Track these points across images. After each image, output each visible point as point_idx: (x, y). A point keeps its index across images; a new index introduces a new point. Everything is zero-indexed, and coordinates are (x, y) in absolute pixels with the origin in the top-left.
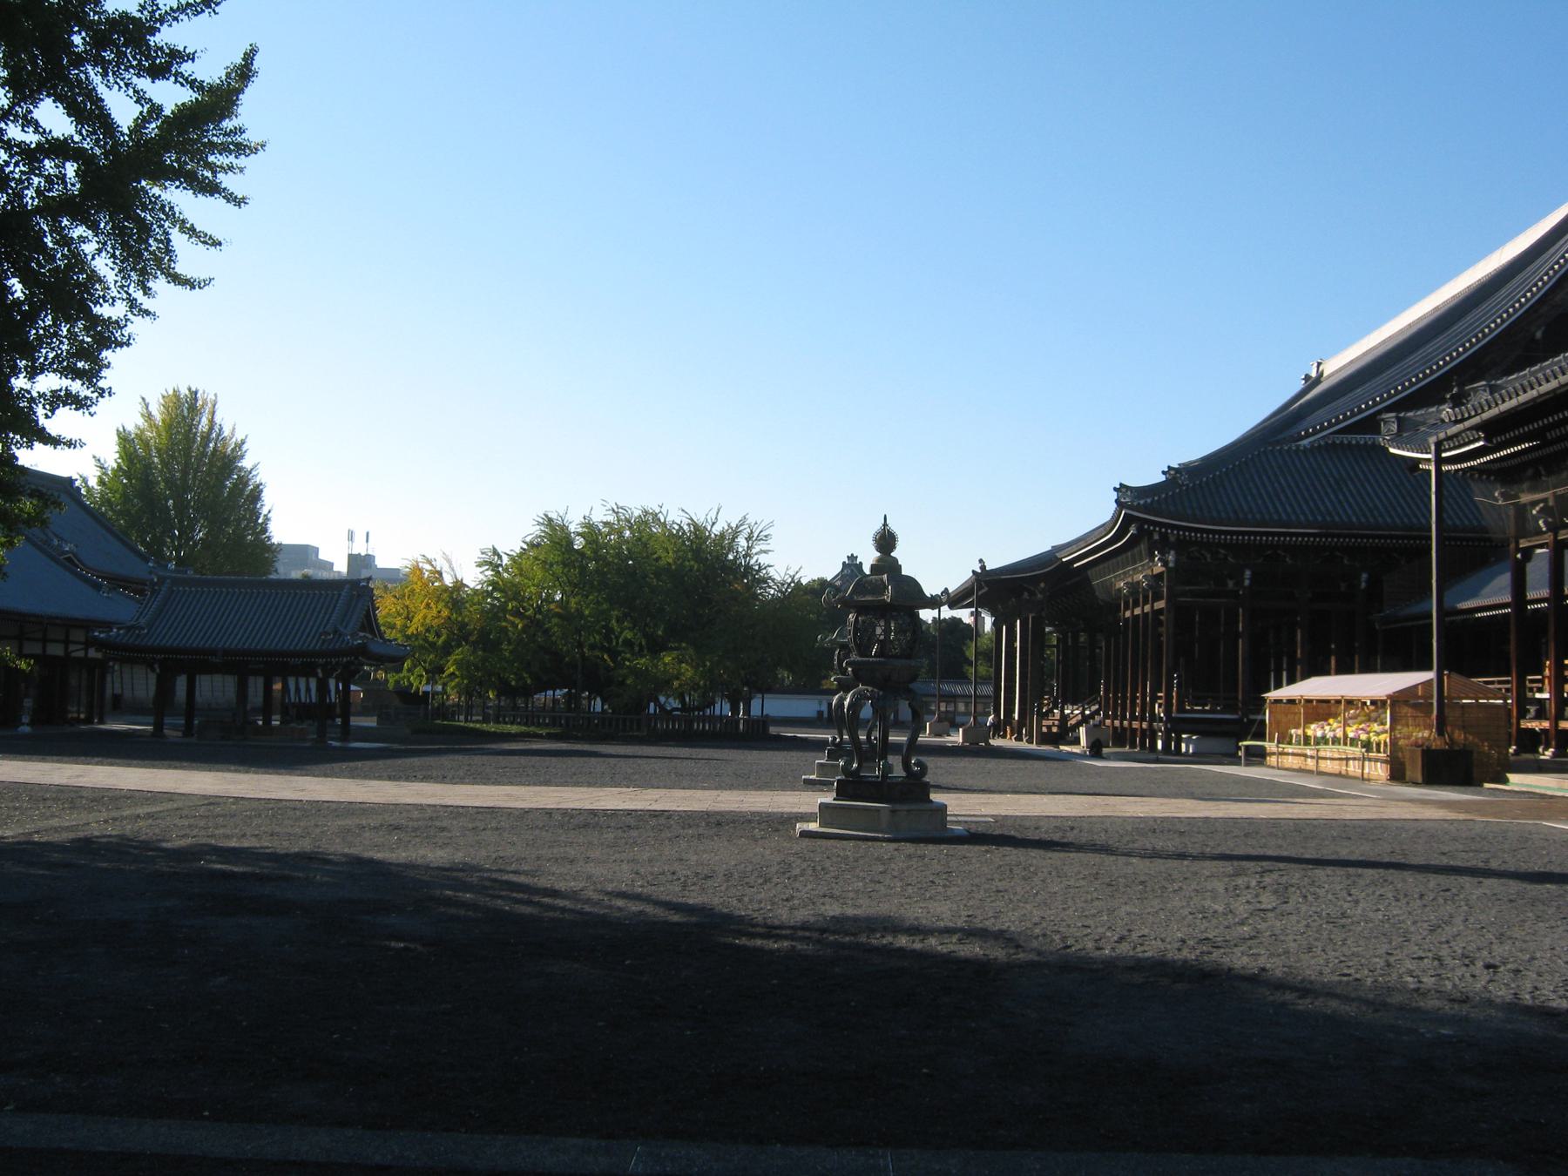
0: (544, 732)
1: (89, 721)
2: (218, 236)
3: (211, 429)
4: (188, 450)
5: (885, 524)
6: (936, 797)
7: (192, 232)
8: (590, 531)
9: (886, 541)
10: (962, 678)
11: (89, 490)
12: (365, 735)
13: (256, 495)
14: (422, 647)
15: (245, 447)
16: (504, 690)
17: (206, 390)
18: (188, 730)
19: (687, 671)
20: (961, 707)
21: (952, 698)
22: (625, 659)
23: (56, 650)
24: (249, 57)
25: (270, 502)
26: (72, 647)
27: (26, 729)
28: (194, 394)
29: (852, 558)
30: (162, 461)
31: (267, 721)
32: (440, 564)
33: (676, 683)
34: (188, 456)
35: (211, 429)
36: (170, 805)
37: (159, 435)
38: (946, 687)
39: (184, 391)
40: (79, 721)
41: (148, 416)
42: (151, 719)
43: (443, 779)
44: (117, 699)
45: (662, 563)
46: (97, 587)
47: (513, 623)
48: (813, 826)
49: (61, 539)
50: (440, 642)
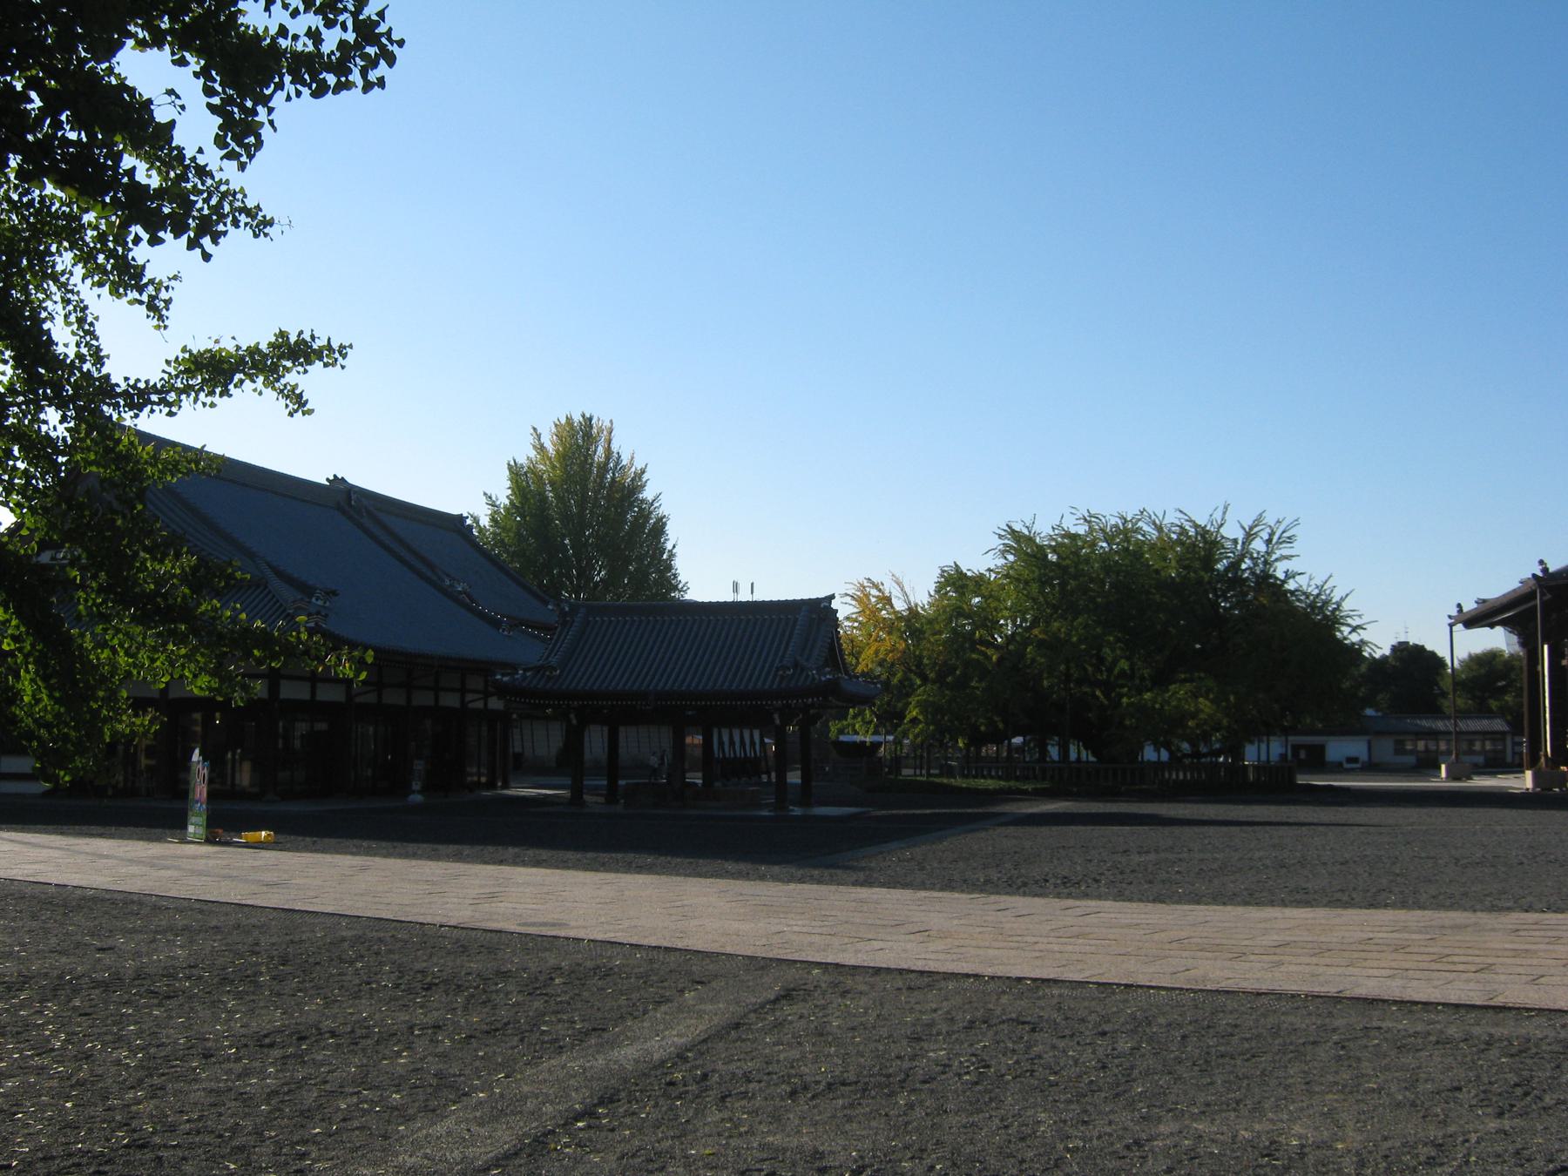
0: (1029, 787)
1: (491, 785)
4: (584, 480)
10: (1435, 711)
11: (481, 530)
13: (659, 528)
15: (645, 478)
16: (977, 740)
17: (602, 416)
18: (612, 794)
20: (1443, 746)
21: (1434, 734)
22: (1122, 696)
23: (450, 700)
25: (674, 535)
26: (469, 697)
30: (557, 496)
32: (890, 588)
34: (585, 489)
37: (554, 467)
38: (1426, 723)
39: (577, 418)
41: (541, 448)
42: (568, 781)
44: (518, 757)
47: (984, 654)
50: (895, 681)
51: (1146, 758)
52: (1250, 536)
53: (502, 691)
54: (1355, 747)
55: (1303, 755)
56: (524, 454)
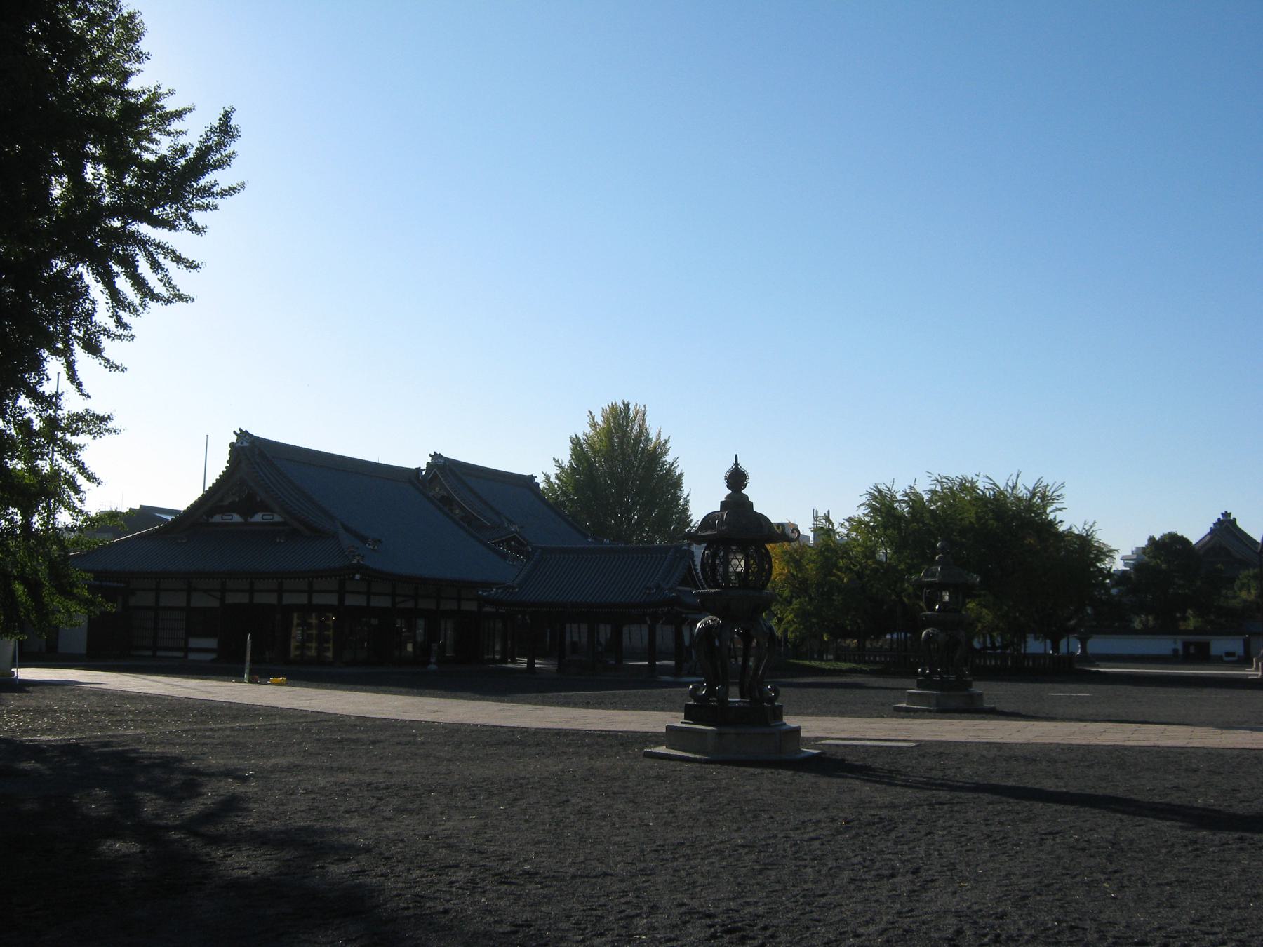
1: (506, 662)
3: (641, 432)
5: (736, 463)
6: (790, 721)
7: (177, 259)
8: (914, 499)
9: (737, 478)
13: (676, 483)
15: (668, 445)
24: (226, 117)
25: (687, 487)
28: (627, 406)
29: (1226, 515)
33: (979, 626)
36: (260, 722)
40: (494, 661)
43: (588, 705)
46: (504, 557)
48: (662, 750)
49: (510, 521)
51: (1029, 651)
52: (1034, 495)
54: (1234, 645)
55: (1192, 650)
56: (583, 430)
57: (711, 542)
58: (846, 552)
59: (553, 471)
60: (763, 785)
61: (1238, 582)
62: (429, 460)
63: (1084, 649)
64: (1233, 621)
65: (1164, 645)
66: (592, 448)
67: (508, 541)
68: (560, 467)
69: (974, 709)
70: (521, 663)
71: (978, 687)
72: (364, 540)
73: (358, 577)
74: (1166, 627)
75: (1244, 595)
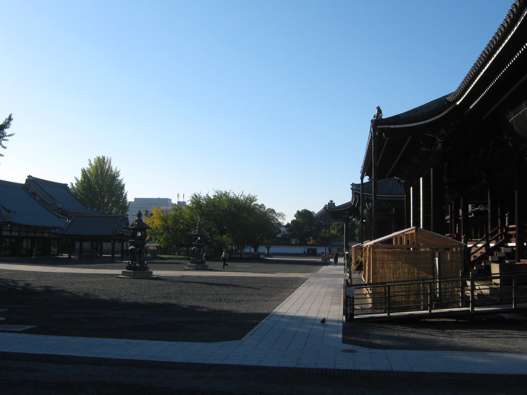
1: (59, 255)
2: (3, 154)
3: (109, 168)
12: (118, 258)
13: (122, 188)
14: (157, 233)
19: (230, 240)
24: (10, 116)
25: (126, 189)
27: (34, 257)
29: (331, 201)
31: (101, 255)
34: (102, 176)
35: (109, 168)
40: (54, 255)
45: (224, 208)
46: (59, 217)
53: (54, 234)
55: (310, 252)
56: (86, 166)
57: (134, 229)
58: (183, 217)
59: (74, 182)
60: (144, 282)
61: (331, 227)
62: (27, 178)
63: (268, 251)
64: (325, 242)
65: (301, 250)
66: (90, 173)
67: (58, 210)
68: (77, 180)
69: (206, 269)
70: (66, 256)
71: (207, 263)
72: (10, 212)
73: (9, 225)
74: (302, 243)
75: (333, 232)
